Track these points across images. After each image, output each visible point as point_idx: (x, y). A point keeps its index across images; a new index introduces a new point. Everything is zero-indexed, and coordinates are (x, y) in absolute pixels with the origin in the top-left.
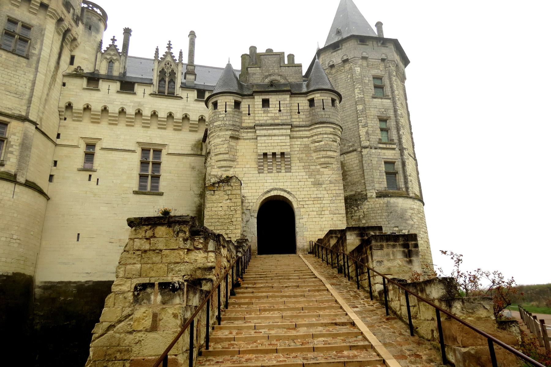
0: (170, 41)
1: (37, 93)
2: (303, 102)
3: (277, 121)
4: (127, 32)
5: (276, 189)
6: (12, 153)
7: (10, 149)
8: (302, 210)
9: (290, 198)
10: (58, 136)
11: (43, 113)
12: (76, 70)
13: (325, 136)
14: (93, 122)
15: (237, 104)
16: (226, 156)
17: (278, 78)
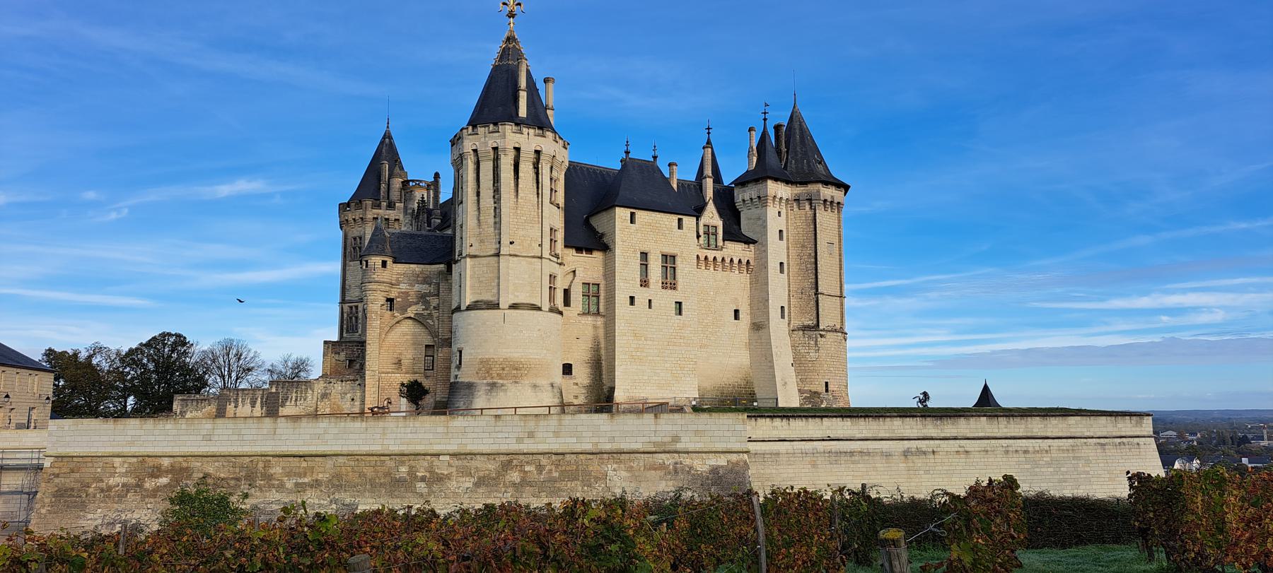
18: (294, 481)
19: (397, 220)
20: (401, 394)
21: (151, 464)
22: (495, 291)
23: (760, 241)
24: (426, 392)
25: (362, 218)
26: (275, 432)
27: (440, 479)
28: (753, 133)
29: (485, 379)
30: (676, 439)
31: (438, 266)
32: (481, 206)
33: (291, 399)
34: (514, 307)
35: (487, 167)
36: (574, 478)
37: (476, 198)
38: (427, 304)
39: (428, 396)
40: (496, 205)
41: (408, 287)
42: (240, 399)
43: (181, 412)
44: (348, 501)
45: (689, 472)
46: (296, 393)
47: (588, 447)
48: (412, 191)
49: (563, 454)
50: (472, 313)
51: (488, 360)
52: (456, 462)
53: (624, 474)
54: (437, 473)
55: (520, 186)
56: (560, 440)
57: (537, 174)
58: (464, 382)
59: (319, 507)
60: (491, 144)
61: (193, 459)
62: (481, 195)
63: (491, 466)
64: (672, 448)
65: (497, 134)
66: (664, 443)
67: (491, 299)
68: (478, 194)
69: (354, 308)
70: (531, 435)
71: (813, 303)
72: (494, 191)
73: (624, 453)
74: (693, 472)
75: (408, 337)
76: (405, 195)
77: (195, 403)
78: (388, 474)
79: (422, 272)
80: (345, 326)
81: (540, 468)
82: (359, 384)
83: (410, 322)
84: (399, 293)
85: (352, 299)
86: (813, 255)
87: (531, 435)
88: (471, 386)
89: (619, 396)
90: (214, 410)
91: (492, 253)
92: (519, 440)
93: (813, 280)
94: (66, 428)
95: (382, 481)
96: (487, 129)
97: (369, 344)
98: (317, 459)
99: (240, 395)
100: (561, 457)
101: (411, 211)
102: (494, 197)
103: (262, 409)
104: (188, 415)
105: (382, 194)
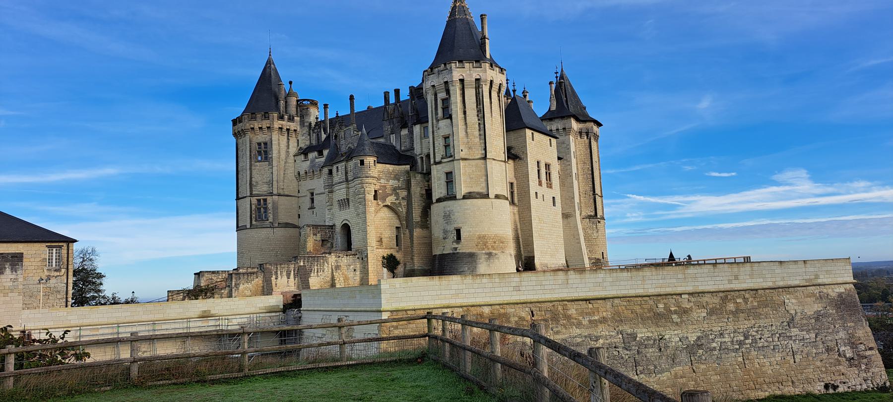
0: (337, 112)
1: (275, 179)
2: (351, 164)
3: (341, 180)
4: (326, 106)
5: (344, 220)
6: (270, 213)
7: (270, 211)
8: (353, 230)
9: (350, 225)
10: (299, 192)
11: (283, 185)
12: (299, 150)
13: (357, 186)
14: (311, 179)
15: (330, 172)
16: (328, 203)
17: (350, 145)
18: (588, 319)
19: (295, 130)
20: (383, 265)
21: (475, 312)
22: (484, 185)
23: (565, 158)
24: (398, 263)
25: (268, 128)
26: (568, 282)
27: (686, 311)
28: (553, 85)
29: (483, 249)
30: (817, 277)
31: (404, 166)
32: (468, 122)
33: (314, 271)
34: (497, 197)
35: (470, 93)
36: (767, 306)
37: (463, 116)
38: (397, 195)
39: (399, 266)
40: (479, 122)
41: (386, 182)
42: (279, 272)
43: (235, 284)
44: (629, 331)
45: (827, 297)
46: (317, 266)
47: (770, 284)
48: (308, 108)
49: (757, 290)
50: (469, 201)
51: (484, 237)
52: (693, 299)
53: (794, 301)
54: (683, 308)
55: (493, 109)
56: (754, 280)
57: (499, 100)
58: (465, 253)
59: (610, 338)
60: (475, 76)
61: (507, 306)
62: (467, 113)
63: (716, 300)
64: (815, 282)
65: (479, 69)
66: (811, 280)
67: (481, 191)
68: (465, 113)
69: (262, 200)
70: (736, 278)
71: (592, 200)
72: (478, 111)
73: (792, 287)
74: (829, 297)
75: (386, 221)
76: (300, 111)
77: (246, 277)
78: (651, 310)
79: (393, 171)
80: (254, 216)
81: (746, 300)
82: (358, 258)
83: (385, 209)
84: (380, 186)
85: (261, 193)
86: (590, 168)
87: (736, 278)
88: (473, 255)
89: (537, 262)
90: (261, 282)
91: (479, 156)
92: (730, 282)
93: (591, 186)
94: (398, 286)
95: (648, 315)
96: (471, 64)
97: (368, 226)
98: (599, 301)
99: (279, 268)
100: (754, 292)
101: (308, 124)
102: (478, 116)
103: (295, 280)
104: (241, 287)
105: (282, 109)
